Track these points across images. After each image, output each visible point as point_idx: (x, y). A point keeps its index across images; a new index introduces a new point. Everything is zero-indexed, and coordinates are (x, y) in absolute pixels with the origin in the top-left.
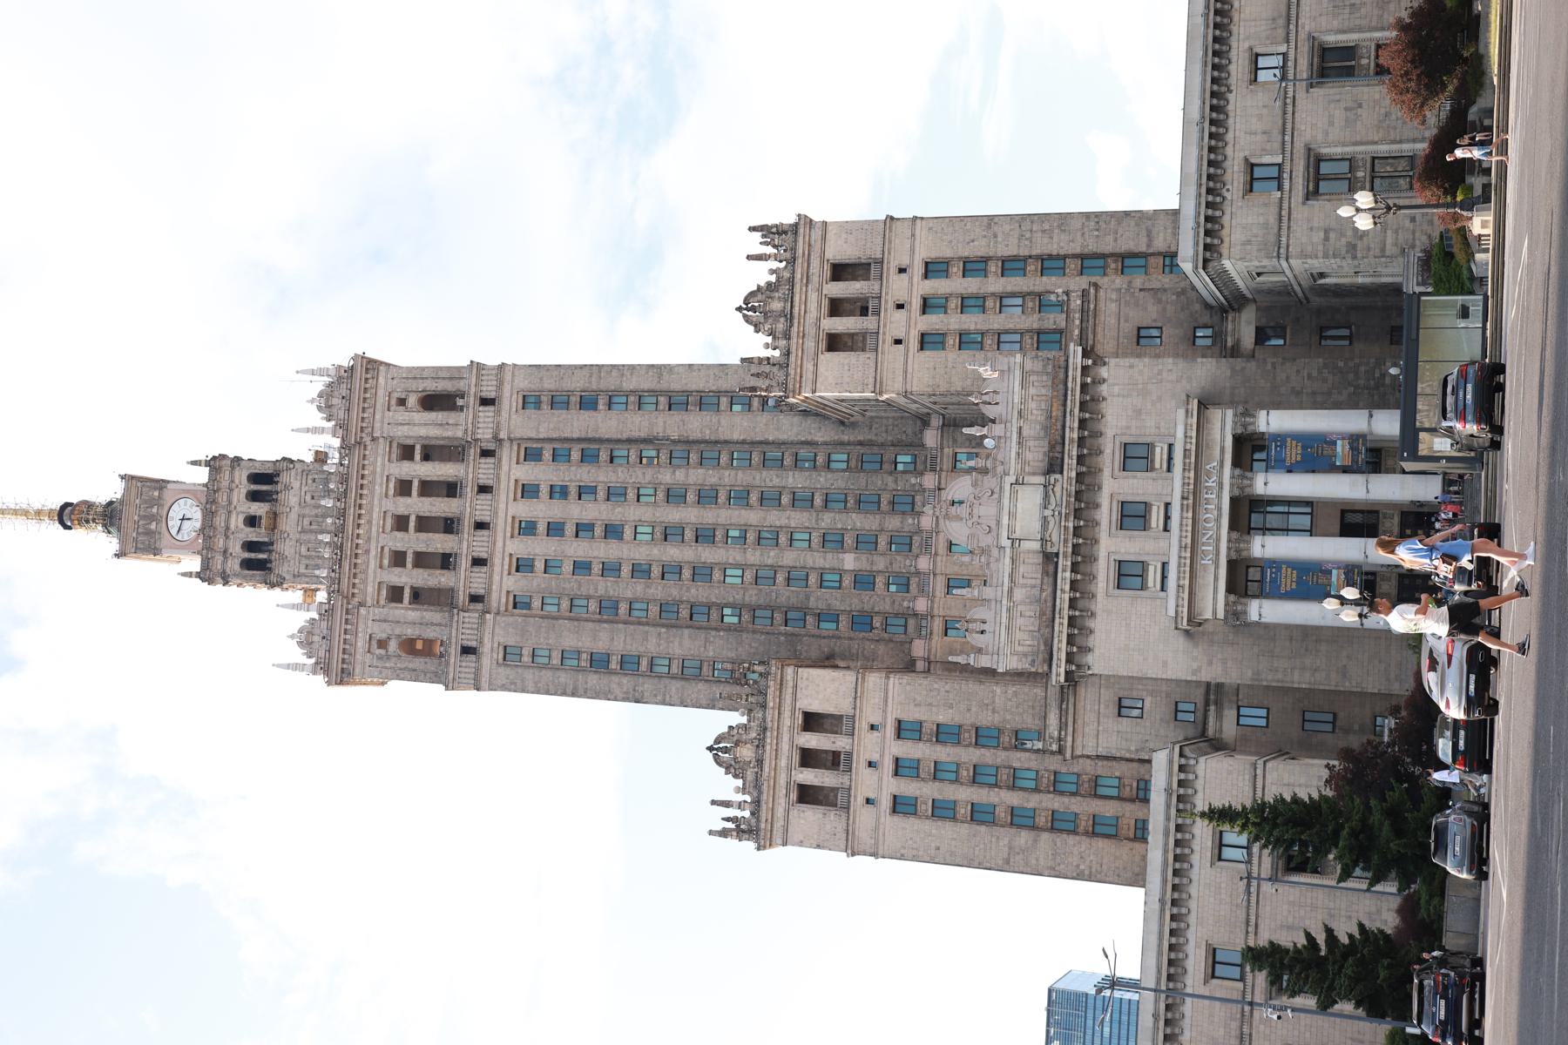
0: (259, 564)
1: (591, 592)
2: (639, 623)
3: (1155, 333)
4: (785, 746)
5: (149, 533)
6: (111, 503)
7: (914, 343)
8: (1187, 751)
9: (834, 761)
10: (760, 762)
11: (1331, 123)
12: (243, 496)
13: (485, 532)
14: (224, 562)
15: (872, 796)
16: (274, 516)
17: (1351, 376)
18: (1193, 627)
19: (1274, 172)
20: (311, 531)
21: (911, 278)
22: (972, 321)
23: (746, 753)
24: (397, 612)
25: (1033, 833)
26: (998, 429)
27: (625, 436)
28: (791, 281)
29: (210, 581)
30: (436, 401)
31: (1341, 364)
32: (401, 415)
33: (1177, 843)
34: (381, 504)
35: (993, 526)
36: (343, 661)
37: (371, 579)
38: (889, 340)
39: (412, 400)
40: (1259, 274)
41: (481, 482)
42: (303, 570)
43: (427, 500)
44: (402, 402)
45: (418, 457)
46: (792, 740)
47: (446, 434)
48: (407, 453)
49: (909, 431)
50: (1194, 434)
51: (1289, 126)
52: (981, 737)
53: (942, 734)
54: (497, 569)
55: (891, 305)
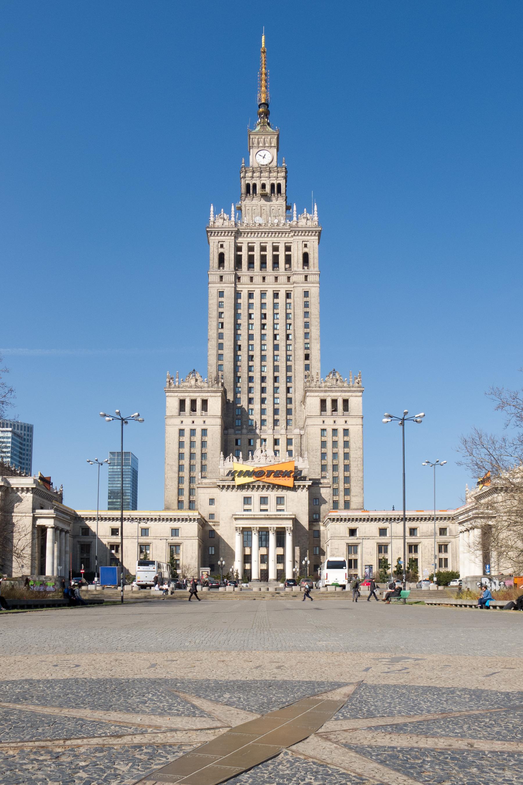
3: (317, 503)
5: (258, 143)
7: (323, 427)
9: (193, 409)
10: (191, 387)
11: (367, 548)
20: (261, 210)
27: (296, 329)
38: (324, 419)
39: (306, 250)
42: (247, 208)
46: (199, 396)
49: (299, 424)
53: (204, 444)
54: (250, 286)
55: (335, 419)
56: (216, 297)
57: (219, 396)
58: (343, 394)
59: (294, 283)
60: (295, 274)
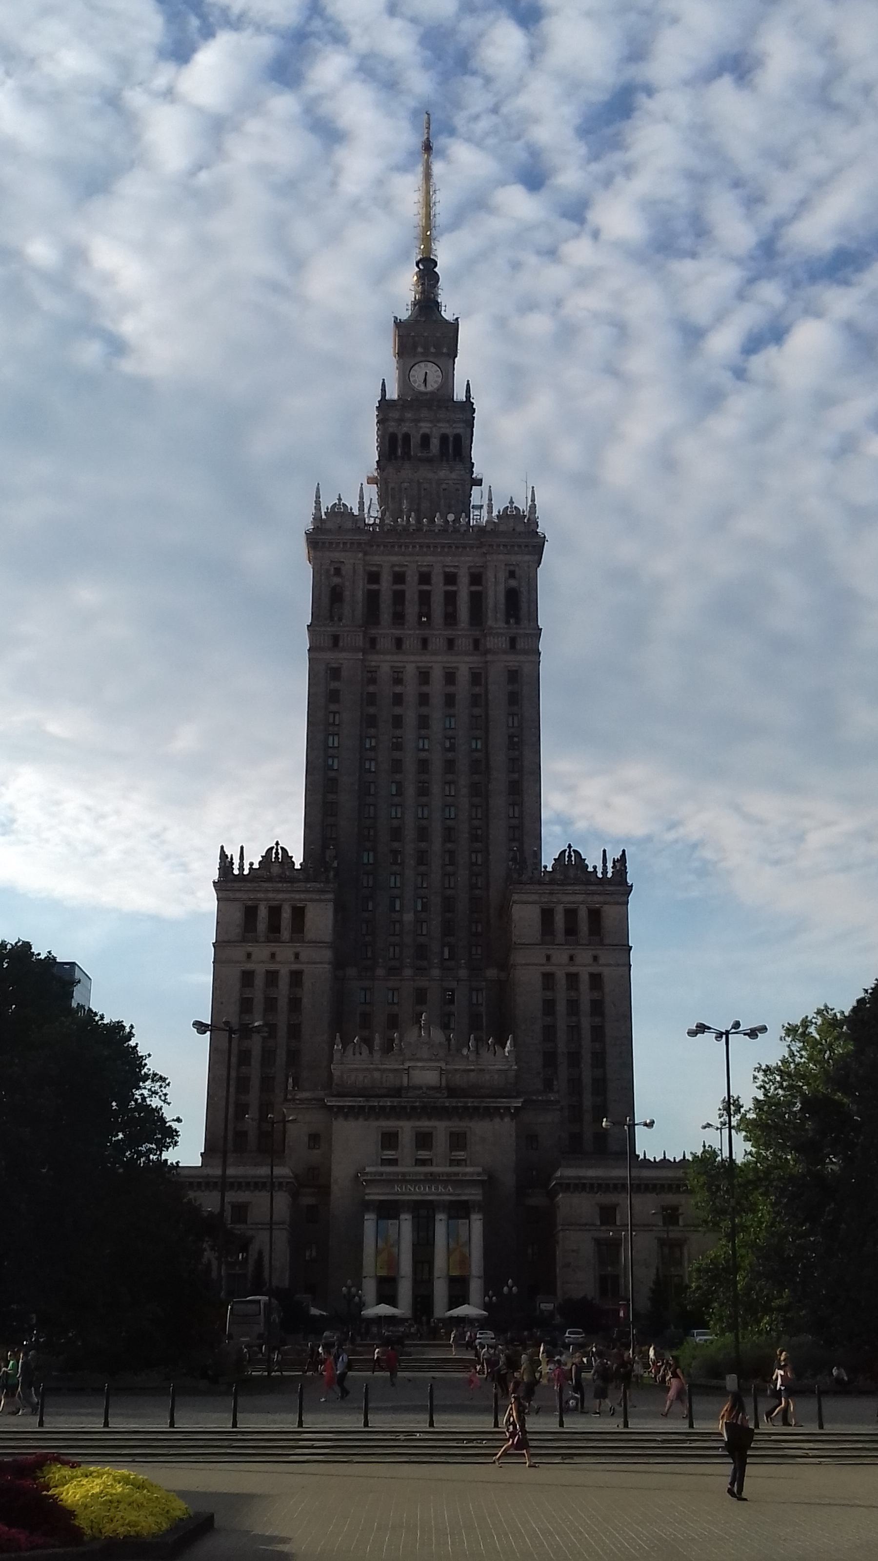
0: (394, 449)
4: (281, 896)
5: (415, 347)
6: (437, 305)
7: (548, 969)
9: (274, 927)
10: (270, 879)
12: (443, 431)
15: (253, 957)
16: (430, 460)
18: (359, 1180)
21: (590, 965)
22: (561, 1008)
23: (275, 870)
26: (472, 1057)
28: (588, 883)
32: (502, 575)
33: (240, 1184)
34: (437, 564)
36: (324, 543)
39: (513, 583)
42: (391, 485)
45: (474, 588)
46: (284, 900)
47: (490, 614)
48: (476, 579)
52: (294, 1031)
54: (395, 658)
57: (329, 900)
59: (486, 652)
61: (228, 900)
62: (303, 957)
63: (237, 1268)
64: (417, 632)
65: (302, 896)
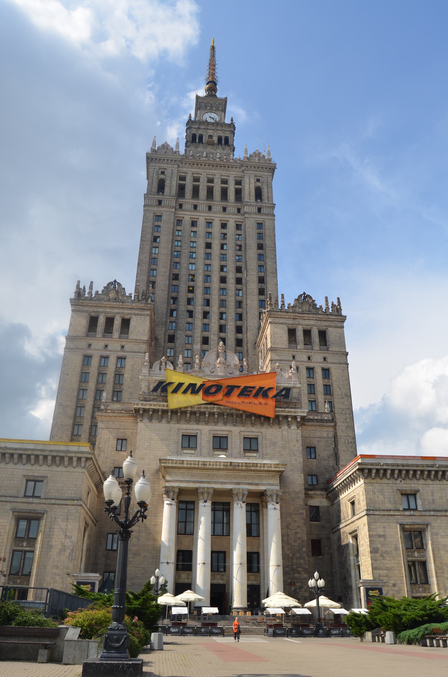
0: (193, 139)
1: (183, 248)
2: (171, 265)
3: (313, 456)
5: (206, 107)
8: (90, 462)
10: (109, 300)
12: (220, 135)
13: (207, 209)
14: (195, 128)
15: (92, 346)
17: (298, 555)
19: (413, 506)
21: (322, 363)
23: (112, 295)
24: (176, 178)
25: (73, 416)
27: (247, 260)
29: (187, 124)
30: (259, 194)
31: (304, 549)
32: (253, 180)
34: (218, 174)
35: (213, 374)
36: (156, 159)
37: (189, 170)
38: (295, 353)
39: (259, 184)
40: (353, 503)
41: (227, 208)
43: (220, 189)
44: (258, 180)
46: (118, 313)
48: (238, 183)
50: (266, 469)
51: (439, 513)
54: (193, 213)
55: (310, 354)
56: (152, 221)
58: (319, 323)
60: (247, 205)
61: (78, 311)
62: (127, 348)
63: (25, 544)
64: (206, 202)
65: (129, 312)
